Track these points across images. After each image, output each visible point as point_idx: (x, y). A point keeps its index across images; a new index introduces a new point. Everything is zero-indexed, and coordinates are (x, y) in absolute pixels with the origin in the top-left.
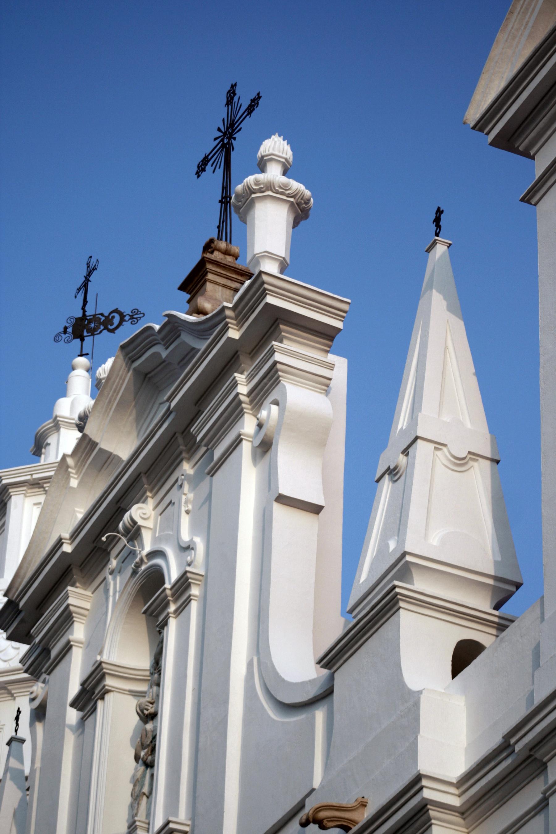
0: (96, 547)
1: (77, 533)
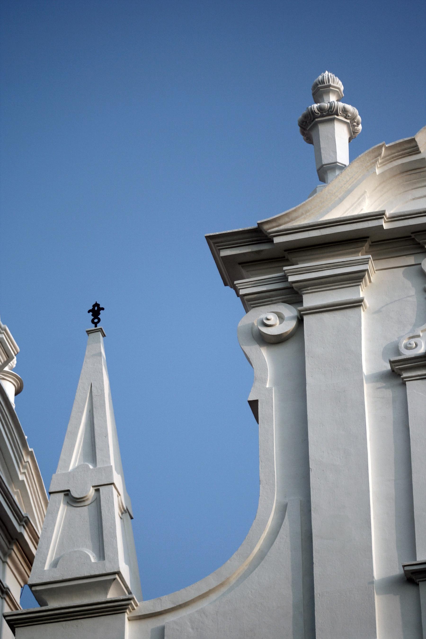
0: (411, 236)
1: (403, 218)
